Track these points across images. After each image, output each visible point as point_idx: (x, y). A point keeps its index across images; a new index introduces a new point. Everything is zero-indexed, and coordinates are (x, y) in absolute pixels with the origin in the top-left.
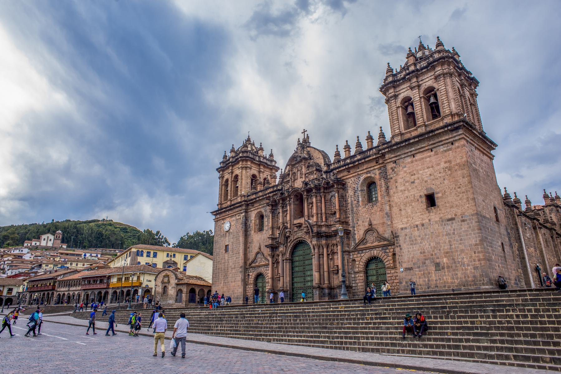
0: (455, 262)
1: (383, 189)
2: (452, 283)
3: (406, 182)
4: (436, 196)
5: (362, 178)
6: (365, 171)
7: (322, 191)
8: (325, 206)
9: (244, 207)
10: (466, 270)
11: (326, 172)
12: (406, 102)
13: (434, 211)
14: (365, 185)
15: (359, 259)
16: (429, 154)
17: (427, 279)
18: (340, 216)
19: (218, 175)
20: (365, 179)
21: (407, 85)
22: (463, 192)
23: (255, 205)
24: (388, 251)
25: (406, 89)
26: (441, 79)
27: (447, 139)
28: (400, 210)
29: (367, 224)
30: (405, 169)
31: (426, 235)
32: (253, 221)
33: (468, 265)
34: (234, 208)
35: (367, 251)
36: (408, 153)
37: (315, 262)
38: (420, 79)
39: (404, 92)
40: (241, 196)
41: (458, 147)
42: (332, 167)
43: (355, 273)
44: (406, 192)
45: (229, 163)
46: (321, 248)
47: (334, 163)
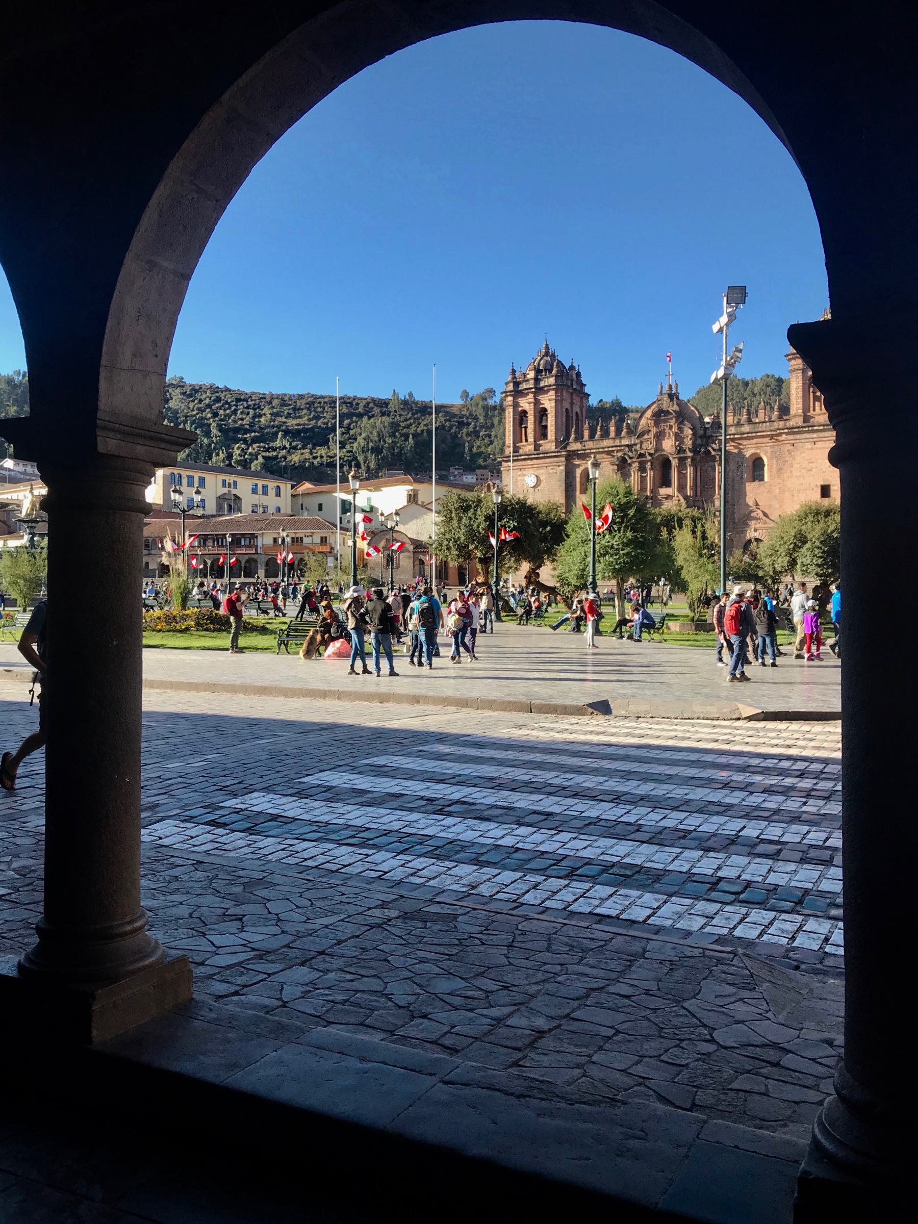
4: (832, 488)
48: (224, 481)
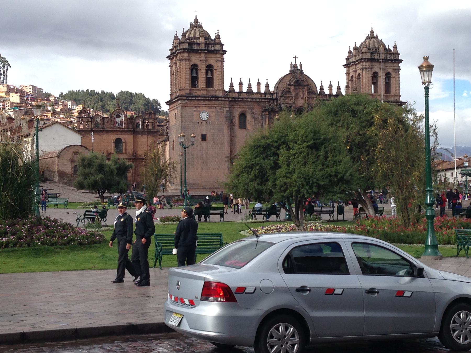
34: (214, 100)
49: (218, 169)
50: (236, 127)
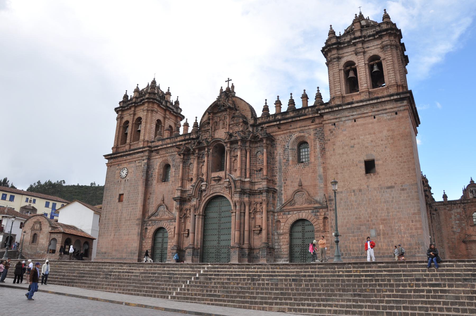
0: (392, 230)
1: (318, 150)
2: (387, 250)
3: (345, 146)
4: (376, 162)
5: (294, 137)
6: (299, 129)
7: (248, 144)
8: (250, 161)
9: (146, 154)
10: (403, 237)
11: (251, 125)
12: (347, 66)
13: (374, 177)
14: (296, 144)
15: (284, 220)
16: (371, 121)
17: (361, 245)
18: (267, 173)
19: (116, 115)
20: (297, 138)
21: (352, 49)
22: (404, 162)
23: (161, 152)
24: (318, 214)
25: (350, 53)
26: (388, 49)
27: (392, 108)
28: (337, 173)
29: (296, 185)
30: (344, 133)
31: (363, 200)
32: (157, 171)
33: (405, 233)
34: (134, 153)
35: (295, 212)
36: (349, 116)
37: (234, 220)
38: (366, 45)
39: (348, 55)
40: (144, 141)
41: (402, 117)
42: (258, 122)
43: (279, 235)
44: (345, 155)
45: (132, 104)
46: (243, 206)
47: (262, 117)
48: (27, 199)
49: (128, 235)
50: (155, 182)
